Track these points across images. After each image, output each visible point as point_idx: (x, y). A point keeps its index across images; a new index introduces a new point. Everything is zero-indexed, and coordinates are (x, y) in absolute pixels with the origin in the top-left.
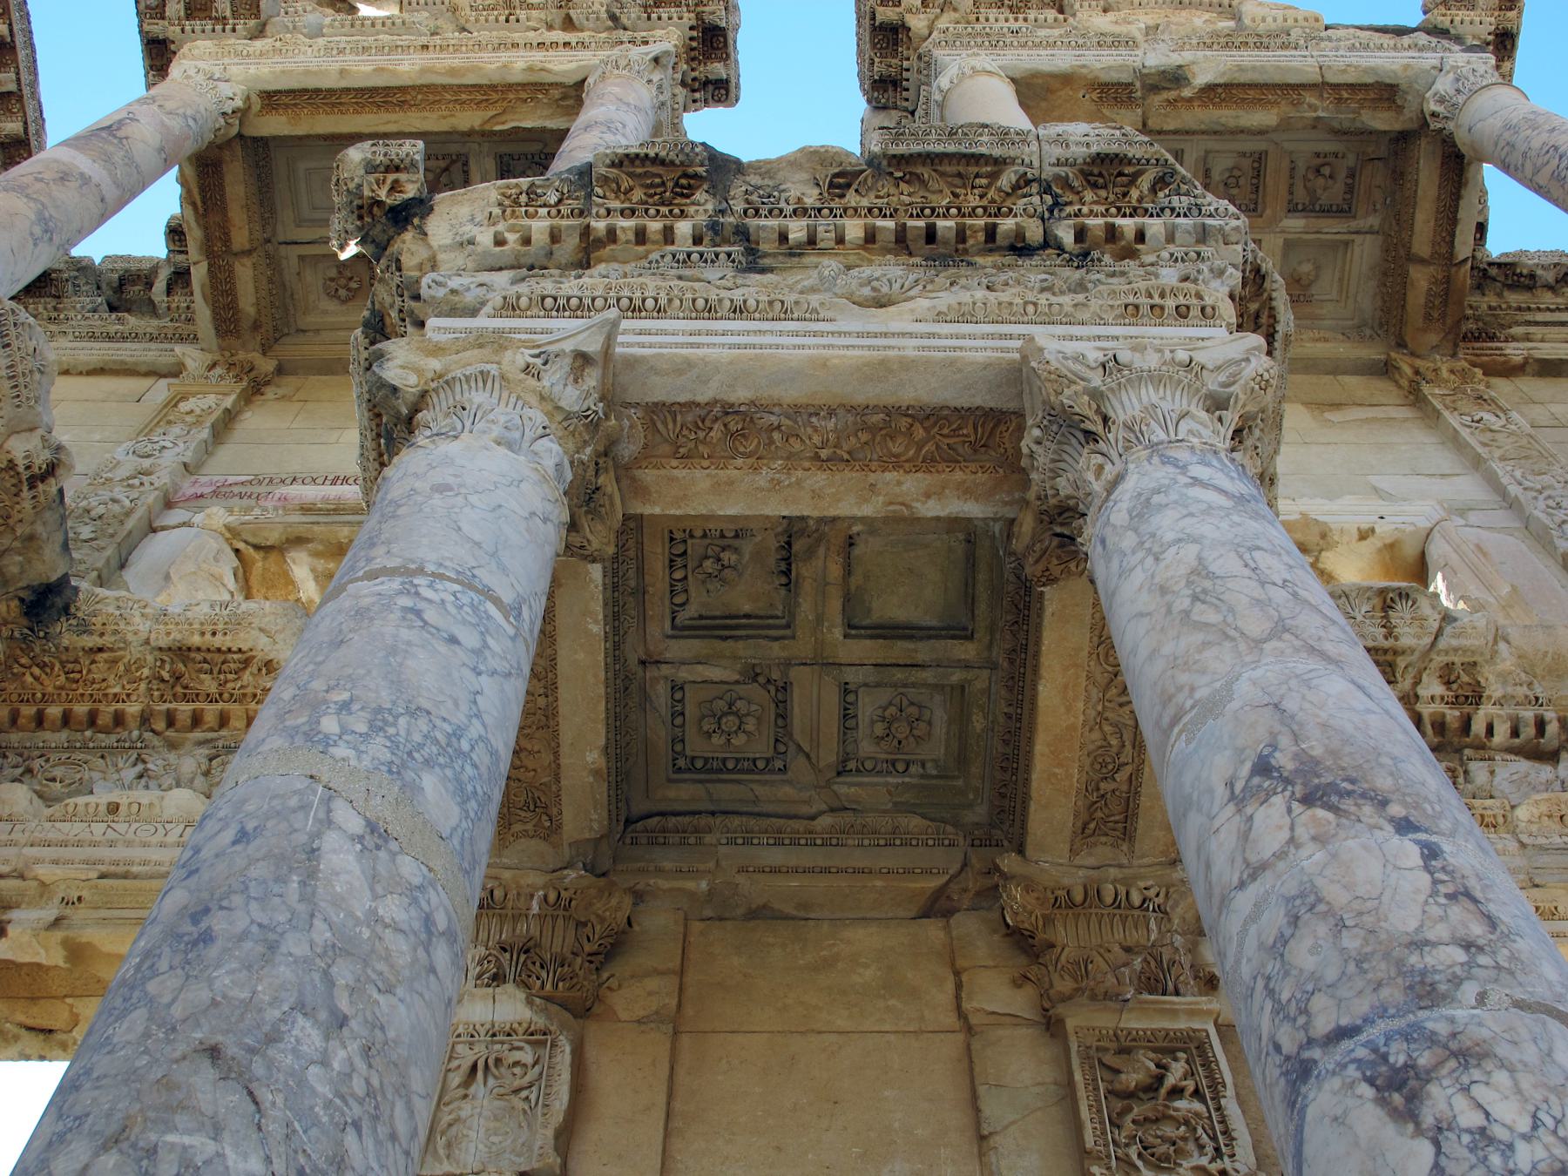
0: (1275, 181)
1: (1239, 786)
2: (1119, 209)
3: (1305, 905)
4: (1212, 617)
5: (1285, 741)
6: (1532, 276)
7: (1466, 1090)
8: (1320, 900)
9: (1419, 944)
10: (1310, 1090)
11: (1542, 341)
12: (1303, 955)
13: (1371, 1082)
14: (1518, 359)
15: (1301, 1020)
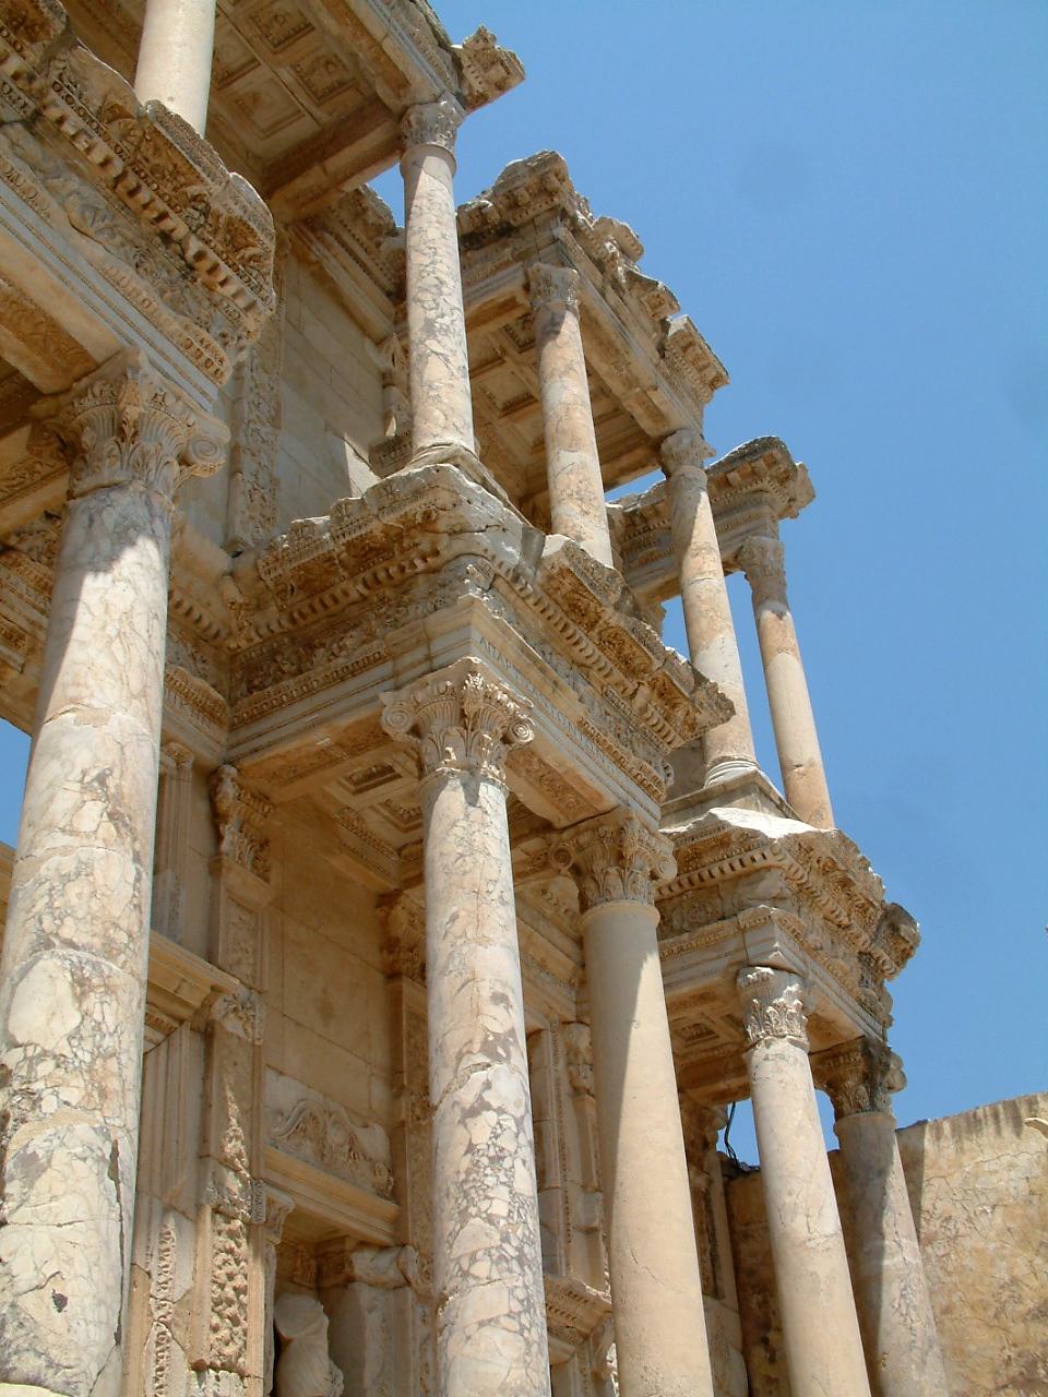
0: (303, 45)
1: (87, 779)
2: (228, 257)
3: (84, 870)
4: (120, 656)
5: (117, 773)
6: (365, 210)
7: (102, 1003)
8: (92, 874)
9: (116, 926)
10: (46, 955)
11: (335, 256)
12: (73, 890)
13: (73, 974)
14: (313, 258)
15: (58, 922)
